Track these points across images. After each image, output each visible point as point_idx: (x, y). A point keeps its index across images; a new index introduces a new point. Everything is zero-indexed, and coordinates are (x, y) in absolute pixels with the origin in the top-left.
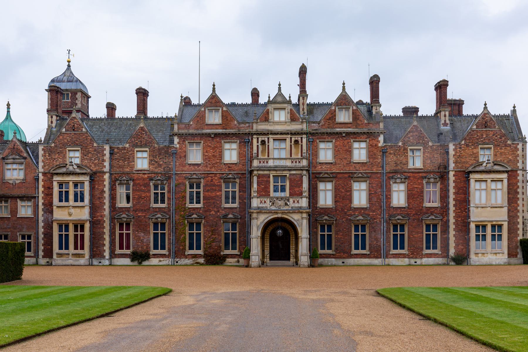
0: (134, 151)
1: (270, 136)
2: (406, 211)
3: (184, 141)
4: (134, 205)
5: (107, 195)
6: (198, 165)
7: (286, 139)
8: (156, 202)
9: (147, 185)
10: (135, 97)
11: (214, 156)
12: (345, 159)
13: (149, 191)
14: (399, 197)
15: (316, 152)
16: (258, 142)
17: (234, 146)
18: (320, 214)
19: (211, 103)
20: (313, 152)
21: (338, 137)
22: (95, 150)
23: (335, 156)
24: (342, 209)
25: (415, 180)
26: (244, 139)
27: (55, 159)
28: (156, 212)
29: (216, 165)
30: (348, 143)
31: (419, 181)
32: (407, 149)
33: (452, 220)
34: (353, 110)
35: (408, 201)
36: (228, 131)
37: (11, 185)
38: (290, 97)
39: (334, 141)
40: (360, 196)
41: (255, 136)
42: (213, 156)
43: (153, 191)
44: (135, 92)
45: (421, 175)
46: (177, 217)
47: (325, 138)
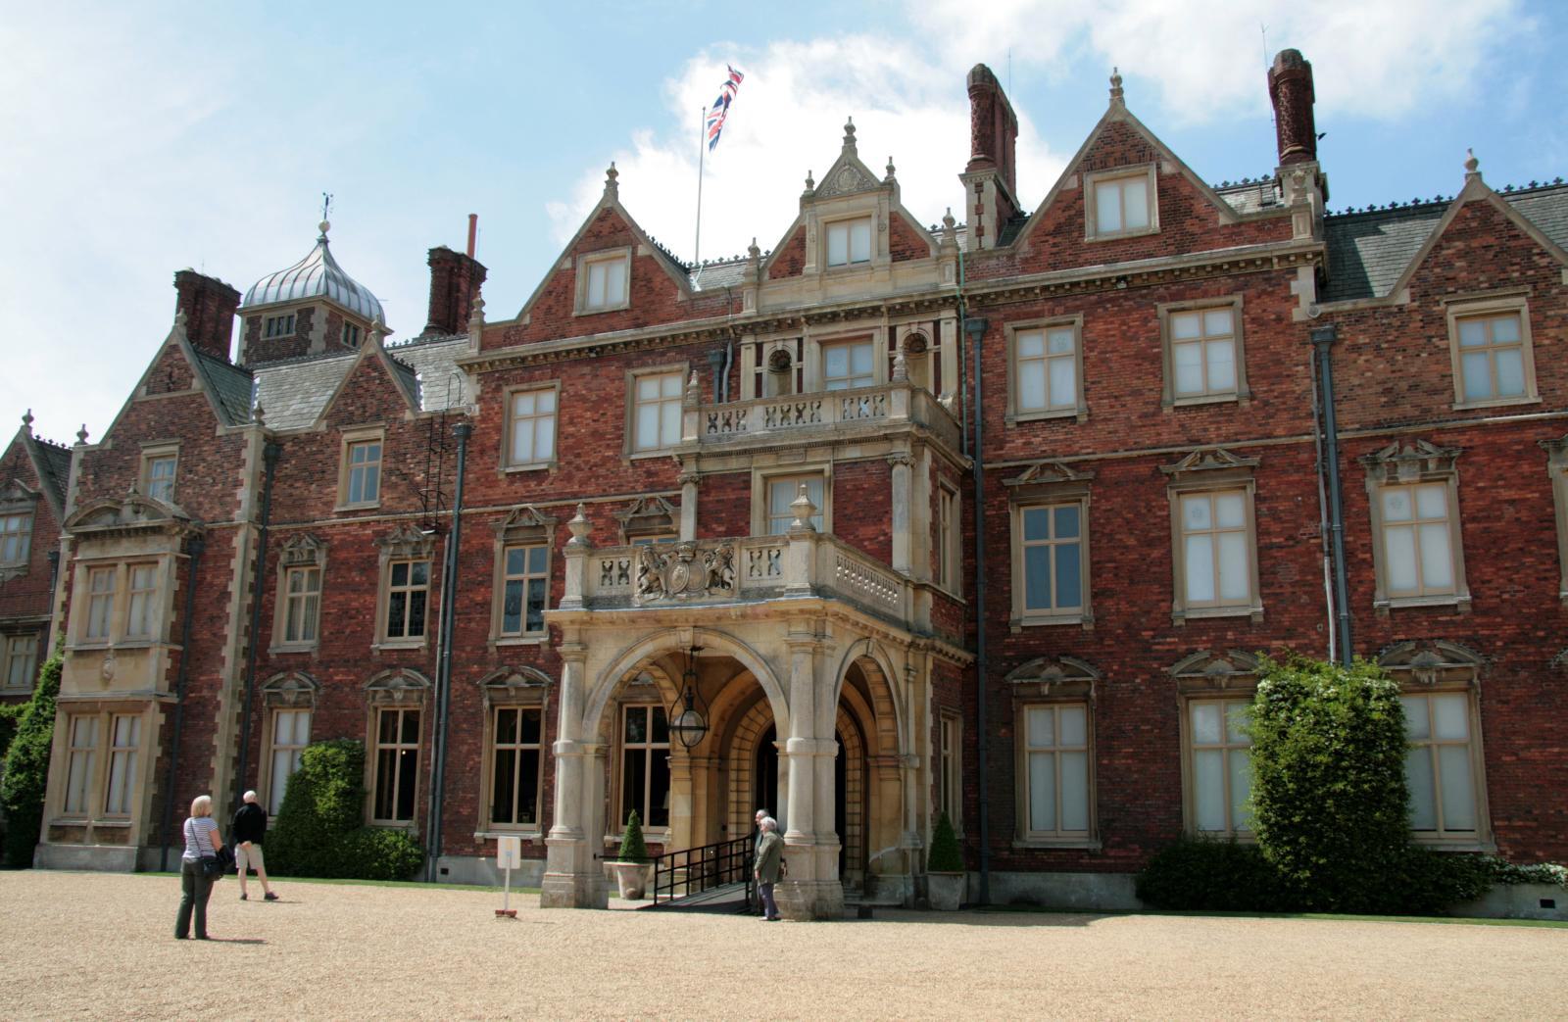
0: (339, 445)
1: (807, 331)
2: (1462, 625)
3: (498, 389)
4: (324, 643)
6: (538, 475)
7: (871, 337)
8: (395, 630)
9: (370, 566)
12: (1137, 393)
13: (372, 588)
15: (1003, 375)
16: (759, 363)
18: (1027, 655)
20: (990, 376)
21: (1100, 303)
23: (1086, 390)
24: (1128, 627)
28: (390, 666)
29: (602, 471)
30: (1145, 320)
31: (1526, 468)
34: (1160, 178)
35: (1468, 572)
38: (891, 169)
39: (1079, 319)
40: (1215, 561)
41: (748, 339)
42: (597, 435)
43: (387, 588)
45: (1530, 435)
46: (456, 685)
47: (1038, 315)
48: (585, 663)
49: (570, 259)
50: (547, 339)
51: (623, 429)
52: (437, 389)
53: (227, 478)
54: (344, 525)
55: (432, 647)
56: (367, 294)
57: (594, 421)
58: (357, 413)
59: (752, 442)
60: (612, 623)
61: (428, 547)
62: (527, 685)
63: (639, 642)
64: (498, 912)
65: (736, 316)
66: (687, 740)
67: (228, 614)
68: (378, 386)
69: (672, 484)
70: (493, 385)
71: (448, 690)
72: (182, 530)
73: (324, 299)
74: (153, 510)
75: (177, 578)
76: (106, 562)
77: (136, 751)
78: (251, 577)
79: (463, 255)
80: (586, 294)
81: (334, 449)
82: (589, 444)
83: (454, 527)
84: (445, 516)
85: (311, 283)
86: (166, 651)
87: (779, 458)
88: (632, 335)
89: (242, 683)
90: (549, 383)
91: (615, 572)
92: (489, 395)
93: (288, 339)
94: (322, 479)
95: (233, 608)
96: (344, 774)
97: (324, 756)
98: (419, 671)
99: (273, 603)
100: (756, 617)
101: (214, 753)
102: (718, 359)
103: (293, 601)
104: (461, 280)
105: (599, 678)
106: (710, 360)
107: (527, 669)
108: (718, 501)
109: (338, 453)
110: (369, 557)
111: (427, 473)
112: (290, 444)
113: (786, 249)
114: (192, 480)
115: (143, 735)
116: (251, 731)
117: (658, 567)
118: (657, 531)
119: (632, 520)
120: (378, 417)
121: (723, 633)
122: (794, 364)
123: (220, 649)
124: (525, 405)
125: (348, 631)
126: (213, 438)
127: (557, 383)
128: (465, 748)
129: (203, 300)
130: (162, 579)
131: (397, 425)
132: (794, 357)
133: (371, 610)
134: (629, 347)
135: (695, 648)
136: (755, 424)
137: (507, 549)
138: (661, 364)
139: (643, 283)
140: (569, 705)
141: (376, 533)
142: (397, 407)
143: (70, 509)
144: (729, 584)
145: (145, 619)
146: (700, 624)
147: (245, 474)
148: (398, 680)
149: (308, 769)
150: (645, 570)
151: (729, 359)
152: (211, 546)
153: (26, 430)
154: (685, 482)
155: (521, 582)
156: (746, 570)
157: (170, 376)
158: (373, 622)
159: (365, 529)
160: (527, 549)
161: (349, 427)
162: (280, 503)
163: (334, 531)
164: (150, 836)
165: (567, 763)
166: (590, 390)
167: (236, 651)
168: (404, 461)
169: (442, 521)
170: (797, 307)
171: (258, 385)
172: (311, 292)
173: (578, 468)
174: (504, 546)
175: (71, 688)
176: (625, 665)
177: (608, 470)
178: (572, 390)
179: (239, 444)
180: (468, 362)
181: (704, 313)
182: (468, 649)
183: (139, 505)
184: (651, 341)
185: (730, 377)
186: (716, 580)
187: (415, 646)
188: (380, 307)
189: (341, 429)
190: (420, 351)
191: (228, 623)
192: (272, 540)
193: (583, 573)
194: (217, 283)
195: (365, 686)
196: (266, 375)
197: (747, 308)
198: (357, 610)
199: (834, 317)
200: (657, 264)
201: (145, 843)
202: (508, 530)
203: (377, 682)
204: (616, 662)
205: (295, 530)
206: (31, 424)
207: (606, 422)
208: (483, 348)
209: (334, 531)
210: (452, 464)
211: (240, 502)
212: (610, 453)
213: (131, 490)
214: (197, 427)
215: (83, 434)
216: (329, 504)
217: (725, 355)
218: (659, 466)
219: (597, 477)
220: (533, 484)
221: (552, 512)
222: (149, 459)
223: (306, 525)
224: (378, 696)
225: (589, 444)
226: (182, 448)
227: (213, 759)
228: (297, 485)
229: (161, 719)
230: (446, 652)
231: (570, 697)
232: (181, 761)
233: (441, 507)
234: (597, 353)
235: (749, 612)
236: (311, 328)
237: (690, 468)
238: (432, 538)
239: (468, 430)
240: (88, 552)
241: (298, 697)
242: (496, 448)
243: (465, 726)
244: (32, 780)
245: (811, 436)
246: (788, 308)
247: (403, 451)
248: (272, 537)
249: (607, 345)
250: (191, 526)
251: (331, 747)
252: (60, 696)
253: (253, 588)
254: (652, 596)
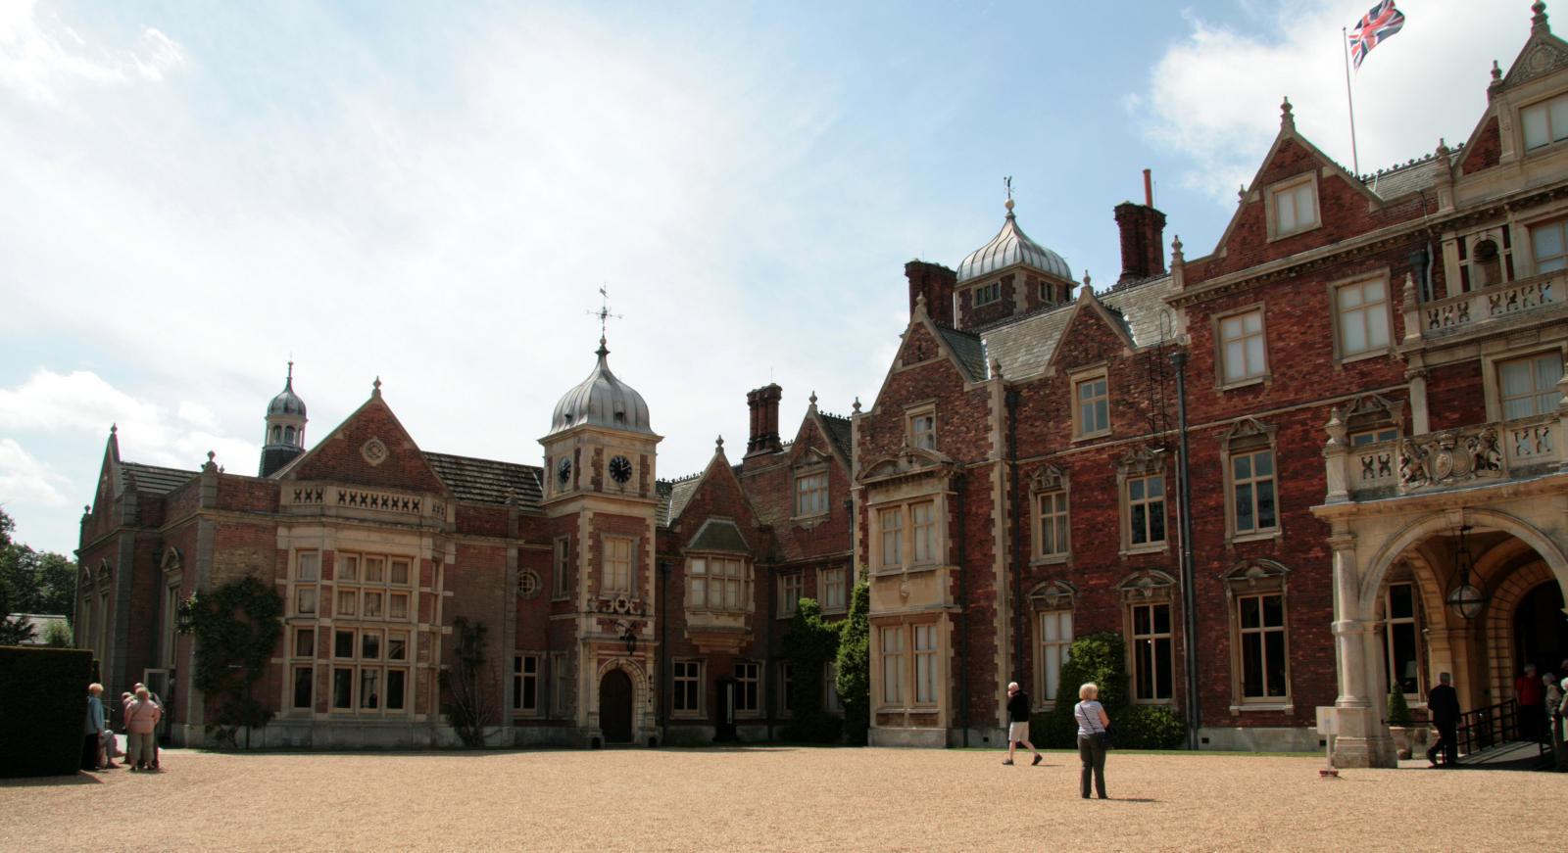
0: (1069, 385)
1: (1511, 218)
3: (1206, 318)
4: (1077, 554)
8: (1139, 538)
9: (1109, 486)
10: (1113, 234)
13: (1114, 503)
16: (1463, 255)
19: (1281, 166)
22: (968, 404)
27: (883, 447)
28: (1139, 569)
29: (1316, 378)
37: (806, 534)
42: (1304, 346)
48: (1355, 550)
49: (1257, 192)
50: (1246, 267)
51: (1330, 337)
52: (1145, 326)
53: (978, 425)
54: (1082, 453)
55: (1173, 549)
56: (1052, 253)
57: (1302, 334)
58: (1080, 356)
59: (1479, 331)
60: (1379, 511)
61: (1160, 464)
62: (1266, 575)
63: (1408, 527)
64: (1322, 772)
65: (1432, 216)
66: (1466, 612)
67: (994, 537)
68: (1094, 331)
69: (1386, 381)
70: (1201, 315)
71: (1193, 585)
72: (949, 472)
73: (1021, 266)
74: (924, 459)
75: (949, 512)
76: (891, 505)
77: (935, 653)
78: (1008, 504)
79: (1144, 207)
80: (1276, 221)
81: (1064, 390)
82: (1299, 355)
83: (1181, 443)
84: (1172, 435)
85: (1008, 253)
86: (948, 572)
87: (1509, 343)
88: (1328, 252)
89: (1012, 593)
90: (1253, 306)
91: (1376, 466)
92: (1199, 324)
93: (996, 304)
94: (1057, 416)
95: (997, 531)
96: (1109, 662)
97: (1090, 648)
98: (1163, 570)
99: (1029, 525)
100: (1529, 493)
101: (996, 651)
102: (1419, 259)
103: (1044, 521)
104: (1146, 228)
105: (1371, 563)
106: (1411, 261)
107: (1265, 562)
108: (1448, 391)
109: (1069, 392)
110: (1108, 477)
111: (1150, 399)
112: (1025, 391)
113: (1478, 143)
114: (949, 430)
115: (938, 640)
116: (1023, 632)
117: (1419, 457)
118: (1376, 426)
119: (1350, 419)
120: (1100, 357)
121: (1494, 511)
122: (1501, 251)
123: (991, 566)
124: (1232, 328)
125: (1097, 542)
126: (962, 394)
127: (1262, 305)
128: (1213, 634)
129: (927, 280)
130: (938, 513)
131: (1118, 363)
132: (1500, 244)
133: (1116, 522)
134: (1328, 262)
135: (1466, 528)
136: (1480, 314)
137: (1233, 457)
138: (1361, 272)
139: (1333, 201)
140: (1345, 589)
141: (1112, 457)
142: (1116, 346)
143: (856, 467)
144: (1496, 466)
145: (928, 546)
146: (1469, 505)
147: (993, 420)
148: (1147, 580)
149: (1077, 660)
150: (1406, 462)
151: (1431, 258)
152: (973, 483)
153: (813, 408)
154: (1412, 377)
155: (1249, 485)
156: (1512, 451)
157: (920, 349)
158: (1118, 532)
159: (1101, 454)
160: (1252, 456)
161: (1076, 369)
162: (1025, 441)
163: (1074, 459)
164: (953, 720)
165: (1349, 640)
166: (1294, 306)
167: (1004, 568)
168: (1129, 391)
169: (1170, 440)
170: (1498, 196)
171: (986, 346)
172: (1009, 262)
173: (1292, 378)
174: (1231, 454)
175: (877, 607)
176: (1395, 550)
177: (1321, 376)
178: (1276, 309)
179: (983, 395)
180: (1175, 298)
181: (1397, 219)
182: (1208, 548)
183: (912, 456)
184: (1348, 253)
185: (1433, 274)
186: (1482, 463)
187: (1158, 550)
188: (1065, 265)
189: (1068, 372)
190: (1121, 296)
191: (994, 544)
192: (1022, 472)
193: (1345, 470)
194: (937, 267)
195: (1118, 587)
196: (990, 337)
197: (1444, 207)
198: (1104, 525)
199: (1542, 199)
200: (1343, 181)
201: (951, 724)
202: (1231, 441)
203: (1128, 582)
204: (1386, 547)
205: (1040, 462)
206: (816, 403)
207: (1313, 334)
208: (1186, 284)
209: (1074, 459)
210: (1172, 388)
211: (992, 444)
212: (1322, 361)
213: (904, 445)
214: (948, 387)
215: (857, 405)
216: (1068, 436)
217: (1426, 255)
218: (1370, 367)
219: (1312, 384)
220: (1250, 398)
221: (1271, 421)
222: (911, 418)
223: (1049, 457)
224: (1129, 595)
225: (1299, 355)
226: (937, 406)
227: (996, 655)
228: (1037, 424)
229: (951, 626)
230: (1188, 553)
231: (1345, 582)
232: (969, 659)
233: (1167, 427)
234: (1296, 272)
235: (1522, 489)
236: (1014, 292)
237: (1416, 364)
238: (1163, 455)
239: (1183, 358)
240: (876, 499)
241: (1059, 601)
242: (1212, 370)
243: (1211, 615)
244: (857, 678)
245: (1543, 317)
246: (1488, 199)
247: (1126, 384)
248: (1021, 469)
249: (1305, 264)
250: (955, 469)
251: (1095, 640)
252: (871, 613)
253: (1010, 514)
254: (1416, 484)
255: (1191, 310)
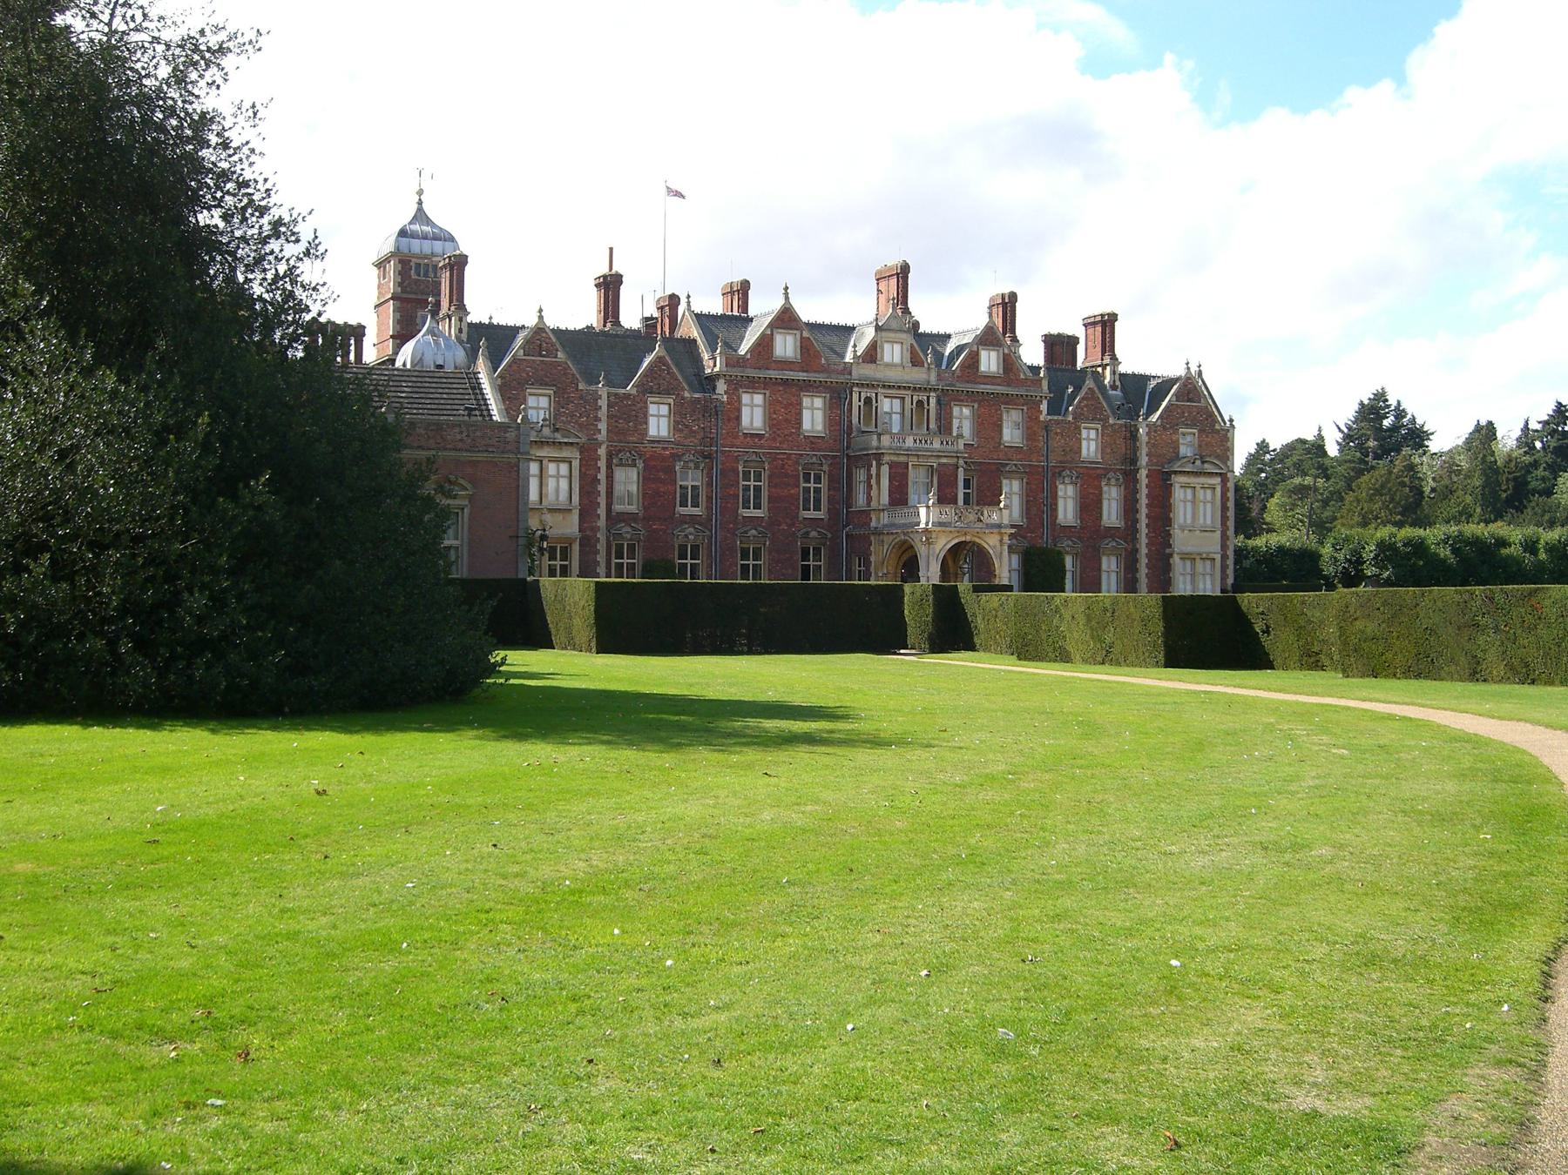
5: (602, 488)
6: (760, 436)
9: (671, 471)
11: (784, 417)
14: (1067, 510)
17: (818, 402)
22: (581, 398)
25: (1090, 481)
26: (838, 395)
32: (1078, 429)
33: (1144, 550)
36: (812, 376)
44: (593, 283)
255: (729, 382)
